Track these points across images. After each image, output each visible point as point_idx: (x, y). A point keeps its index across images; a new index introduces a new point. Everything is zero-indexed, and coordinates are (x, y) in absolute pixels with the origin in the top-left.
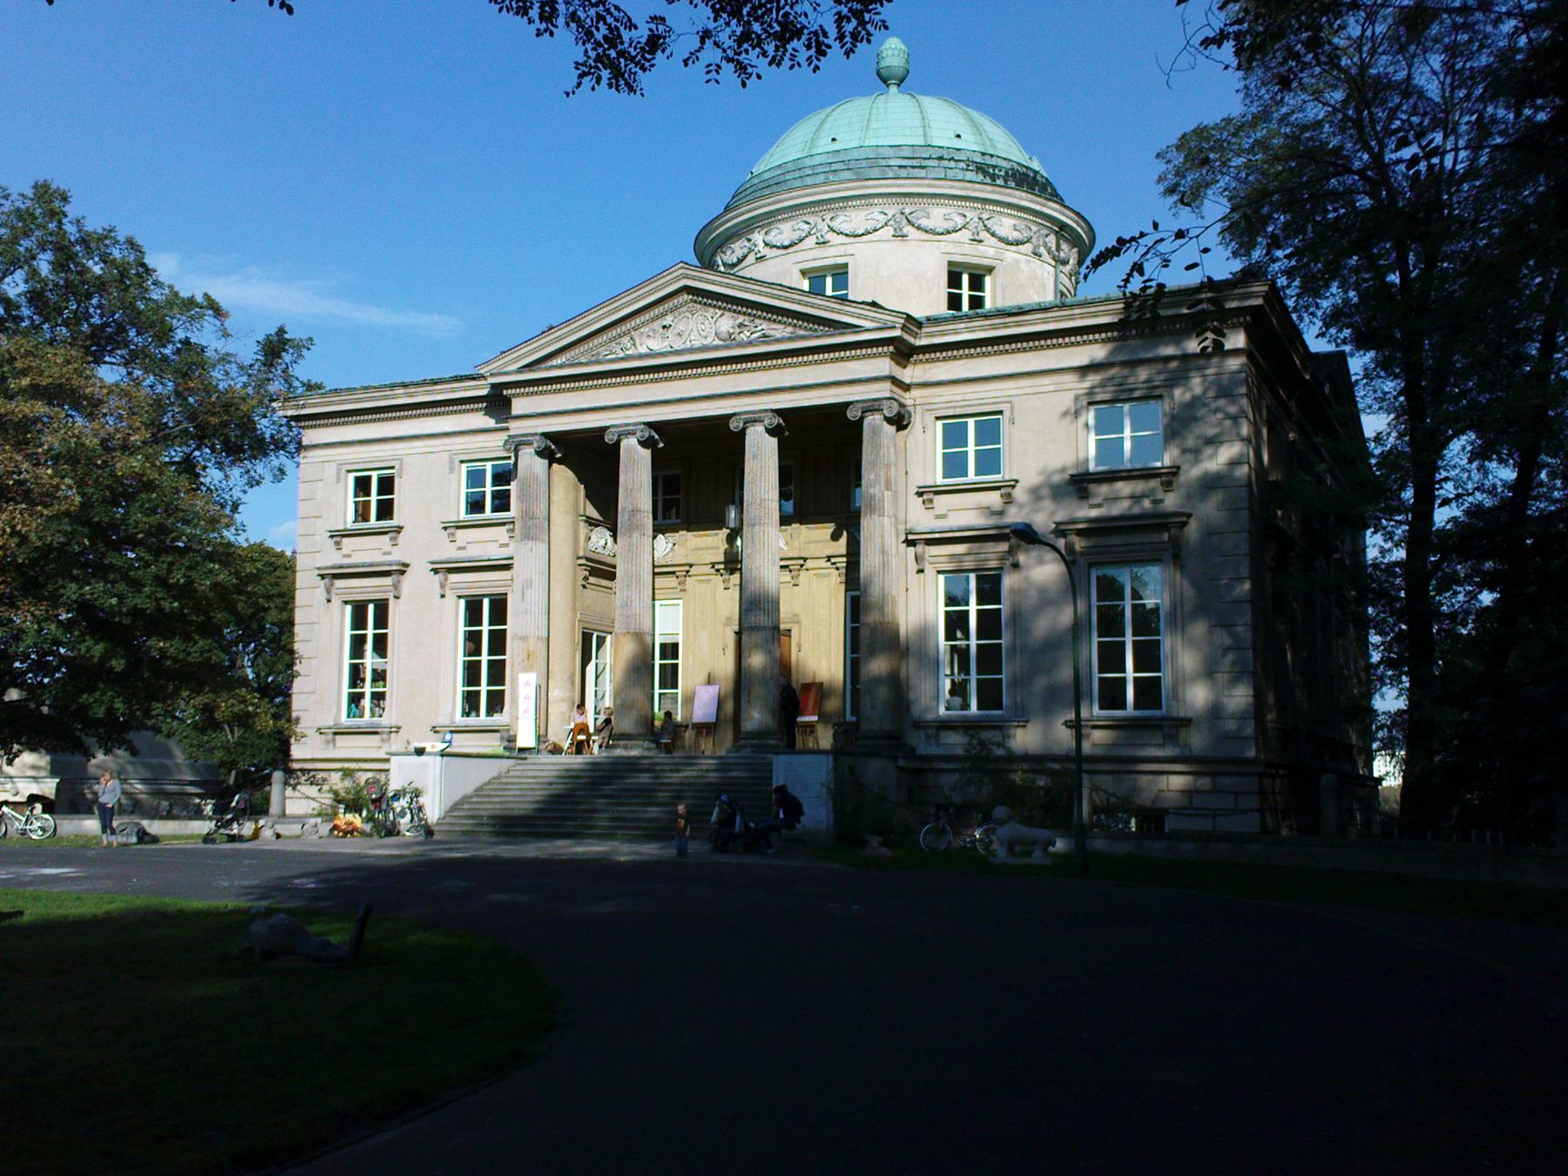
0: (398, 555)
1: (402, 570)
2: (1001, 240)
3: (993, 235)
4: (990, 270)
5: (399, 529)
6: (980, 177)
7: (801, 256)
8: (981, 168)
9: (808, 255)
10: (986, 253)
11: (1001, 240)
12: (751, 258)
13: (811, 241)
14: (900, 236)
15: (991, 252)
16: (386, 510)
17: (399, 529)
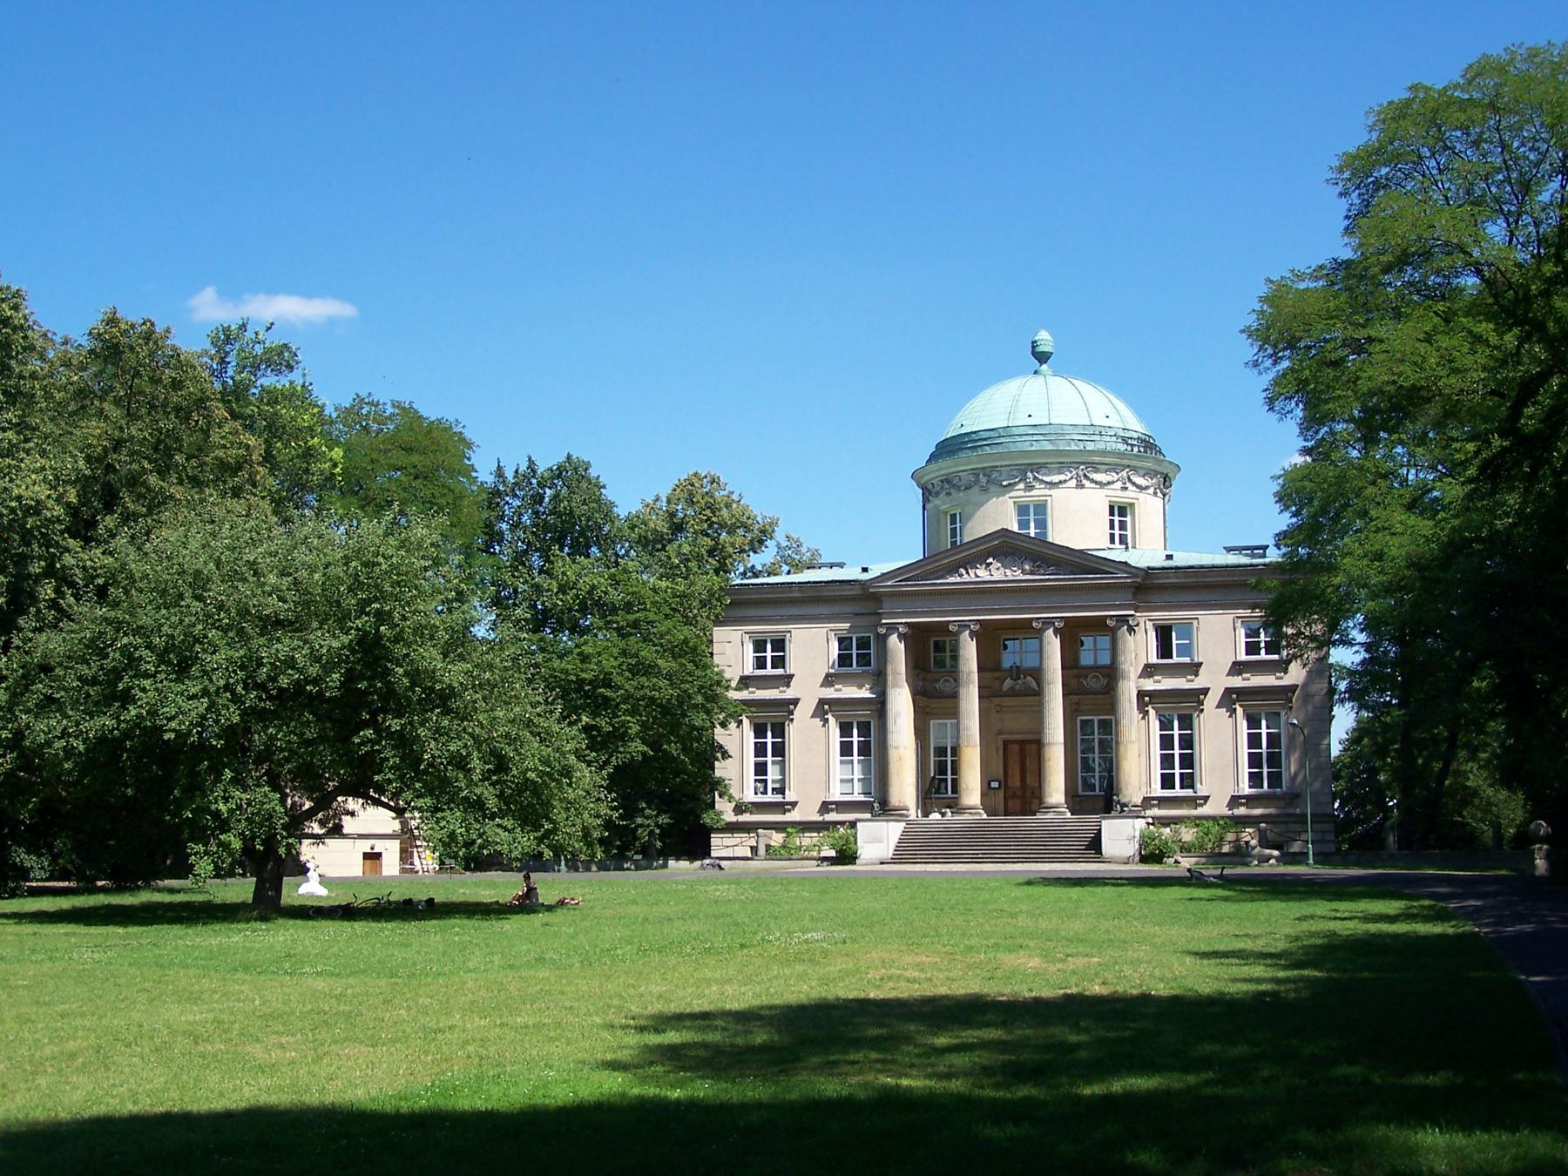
0: (789, 694)
1: (795, 702)
2: (1138, 486)
3: (1134, 484)
4: (1132, 505)
5: (791, 676)
6: (1122, 447)
7: (1014, 494)
8: (1125, 440)
9: (1022, 493)
10: (1131, 494)
11: (1138, 486)
12: (976, 489)
13: (1022, 486)
14: (1080, 486)
15: (1132, 495)
16: (779, 662)
17: (791, 676)
